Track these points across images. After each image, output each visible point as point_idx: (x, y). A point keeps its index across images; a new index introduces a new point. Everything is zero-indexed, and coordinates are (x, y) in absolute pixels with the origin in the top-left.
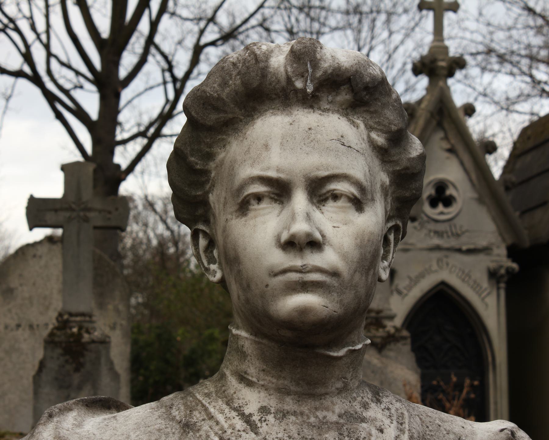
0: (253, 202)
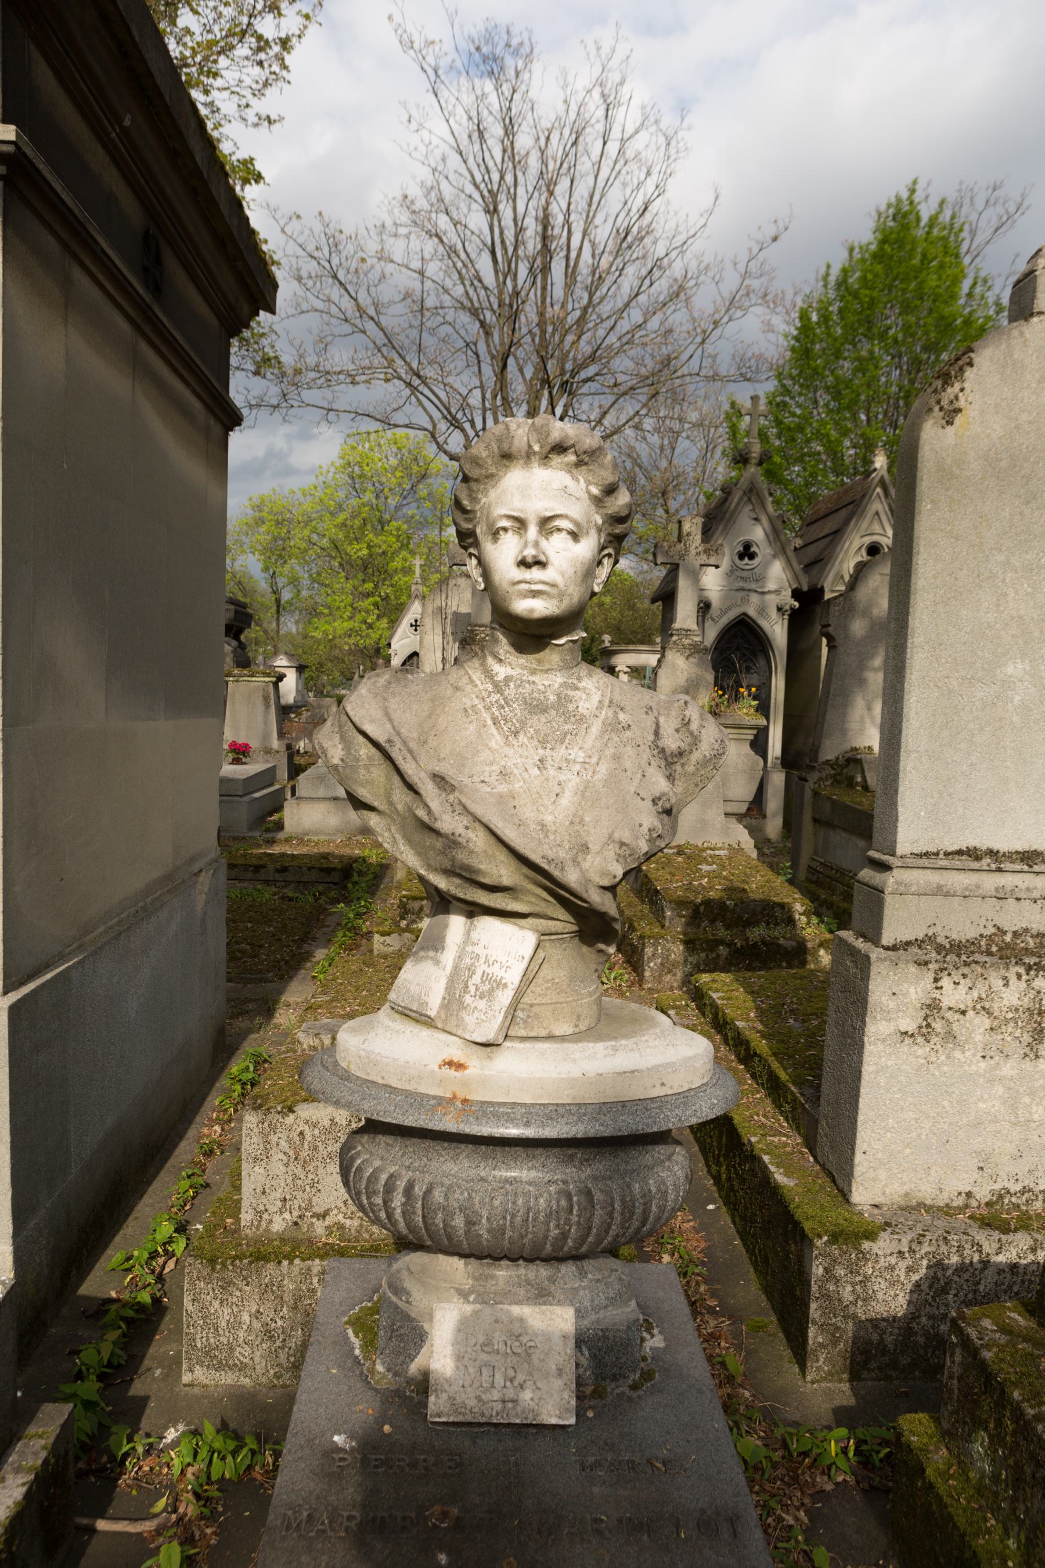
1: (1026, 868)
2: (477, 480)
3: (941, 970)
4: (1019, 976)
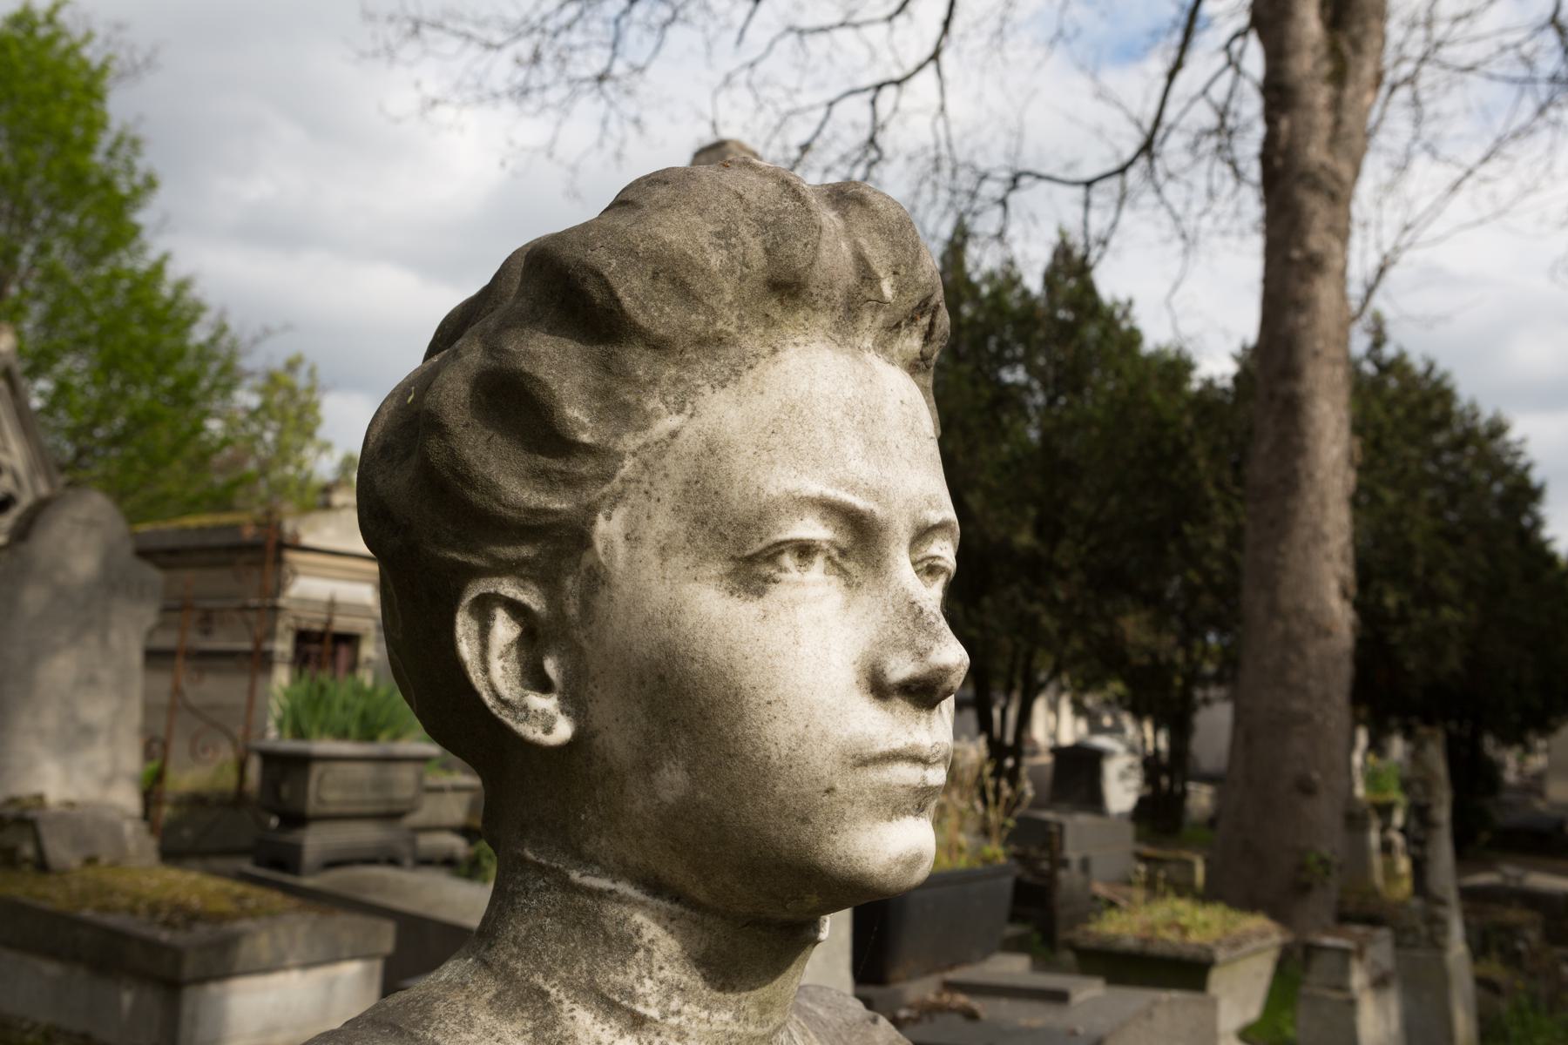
0: (788, 560)
2: (660, 346)
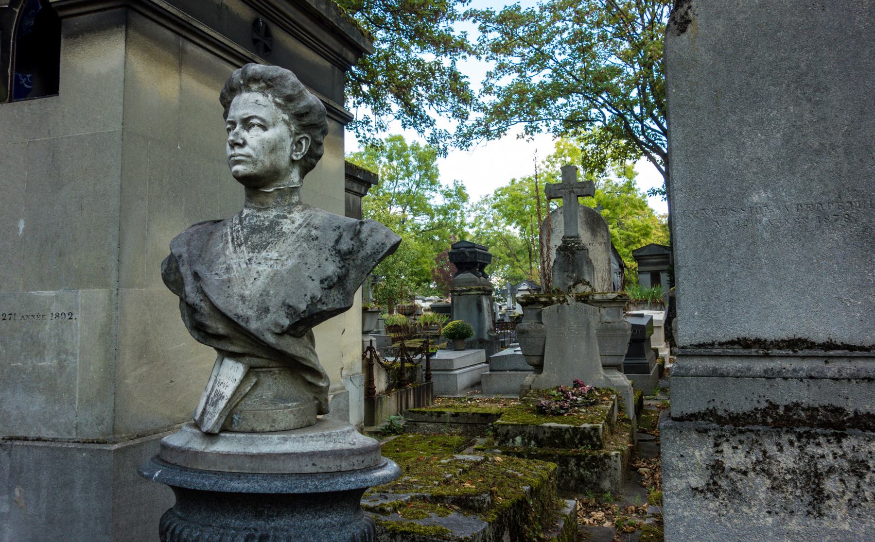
1: (791, 352)
3: (720, 437)
4: (791, 443)
